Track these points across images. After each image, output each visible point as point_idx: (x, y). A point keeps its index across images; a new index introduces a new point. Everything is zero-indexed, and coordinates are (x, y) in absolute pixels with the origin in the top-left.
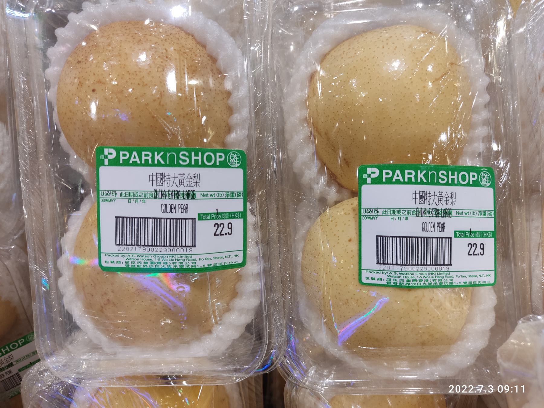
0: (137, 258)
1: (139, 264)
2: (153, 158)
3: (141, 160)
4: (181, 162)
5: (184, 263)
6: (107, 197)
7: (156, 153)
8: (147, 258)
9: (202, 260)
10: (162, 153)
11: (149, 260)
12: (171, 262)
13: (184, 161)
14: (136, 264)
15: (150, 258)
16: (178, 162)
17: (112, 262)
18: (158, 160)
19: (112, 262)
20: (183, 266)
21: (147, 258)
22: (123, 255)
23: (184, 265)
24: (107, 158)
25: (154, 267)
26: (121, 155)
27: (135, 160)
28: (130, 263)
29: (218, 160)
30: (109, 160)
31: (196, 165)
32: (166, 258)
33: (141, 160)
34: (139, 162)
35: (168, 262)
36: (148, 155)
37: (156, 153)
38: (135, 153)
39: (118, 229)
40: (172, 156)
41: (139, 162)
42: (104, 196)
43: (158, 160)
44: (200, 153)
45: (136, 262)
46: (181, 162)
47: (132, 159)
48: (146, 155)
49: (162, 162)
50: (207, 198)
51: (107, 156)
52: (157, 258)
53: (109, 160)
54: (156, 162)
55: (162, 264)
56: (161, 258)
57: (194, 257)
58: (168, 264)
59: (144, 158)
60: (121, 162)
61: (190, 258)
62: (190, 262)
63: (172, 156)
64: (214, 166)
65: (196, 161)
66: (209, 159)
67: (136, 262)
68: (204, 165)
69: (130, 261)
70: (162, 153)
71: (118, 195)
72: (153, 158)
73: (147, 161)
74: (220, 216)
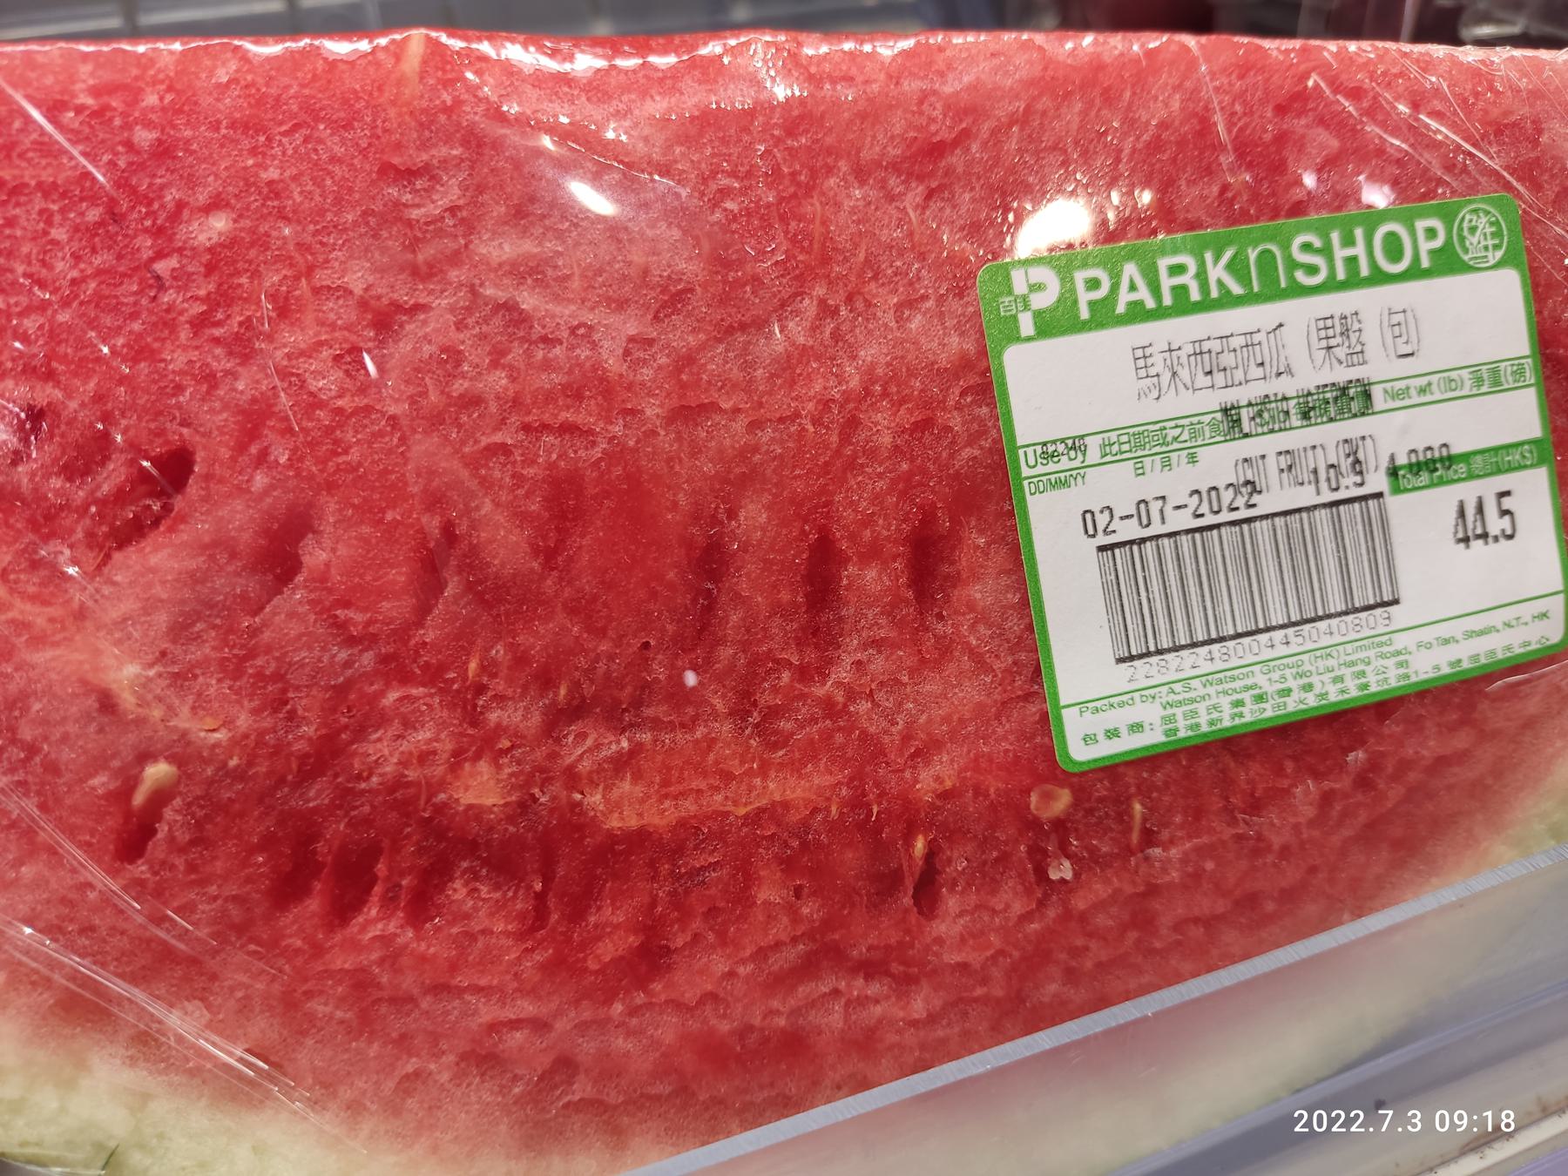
0: (1202, 691)
1: (1215, 715)
2: (1202, 276)
3: (1155, 290)
4: (1300, 276)
5: (1368, 669)
6: (1051, 467)
7: (1208, 256)
8: (1238, 684)
9: (1429, 646)
10: (1228, 254)
11: (1247, 688)
12: (1327, 677)
13: (1312, 270)
14: (1203, 720)
15: (1249, 682)
16: (1292, 278)
17: (1112, 734)
18: (1220, 282)
19: (1112, 734)
20: (1365, 686)
21: (1238, 684)
22: (1146, 693)
23: (1372, 679)
24: (1026, 307)
25: (1269, 714)
26: (1080, 286)
27: (1134, 297)
28: (1180, 717)
29: (1425, 246)
30: (1038, 315)
31: (1353, 281)
32: (1307, 667)
33: (1155, 290)
34: (1150, 304)
35: (1315, 680)
36: (1177, 270)
37: (1208, 256)
38: (1130, 270)
39: (1113, 591)
40: (1266, 259)
41: (1150, 304)
42: (1040, 469)
43: (1220, 282)
44: (1359, 233)
45: (1202, 708)
46: (1300, 276)
47: (1124, 298)
48: (1177, 270)
49: (1237, 289)
50: (1407, 402)
51: (1025, 298)
52: (1276, 676)
53: (1038, 315)
54: (1214, 294)
55: (1295, 695)
56: (1288, 672)
57: (1401, 641)
58: (1318, 689)
59: (1167, 283)
60: (1085, 314)
61: (1385, 649)
62: (1390, 663)
63: (1266, 259)
64: (1415, 273)
65: (1352, 261)
66: (1394, 248)
67: (1202, 708)
68: (1379, 278)
69: (1179, 711)
70: (1228, 254)
71: (1093, 455)
72: (1202, 276)
73: (1180, 291)
74: (1461, 468)
